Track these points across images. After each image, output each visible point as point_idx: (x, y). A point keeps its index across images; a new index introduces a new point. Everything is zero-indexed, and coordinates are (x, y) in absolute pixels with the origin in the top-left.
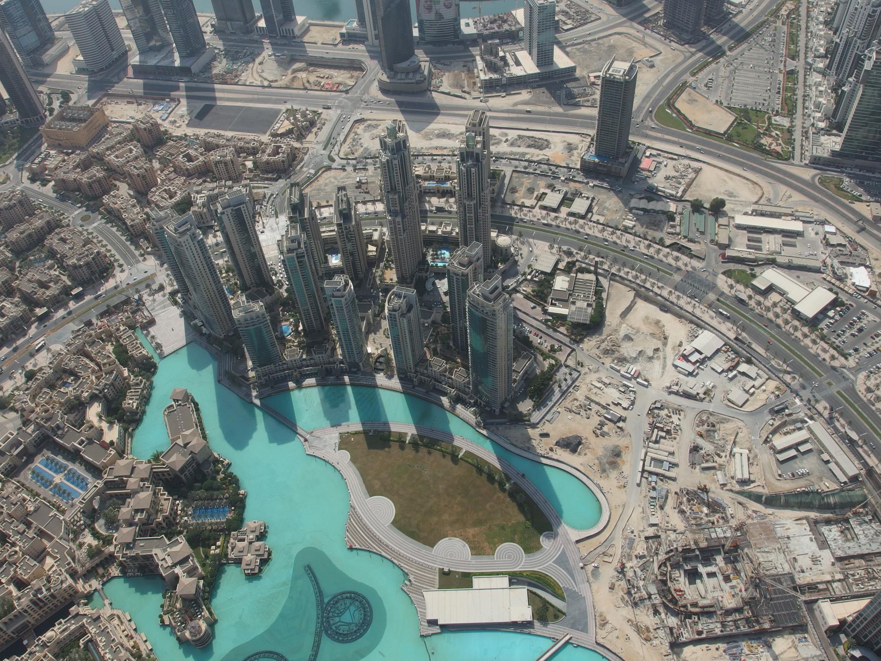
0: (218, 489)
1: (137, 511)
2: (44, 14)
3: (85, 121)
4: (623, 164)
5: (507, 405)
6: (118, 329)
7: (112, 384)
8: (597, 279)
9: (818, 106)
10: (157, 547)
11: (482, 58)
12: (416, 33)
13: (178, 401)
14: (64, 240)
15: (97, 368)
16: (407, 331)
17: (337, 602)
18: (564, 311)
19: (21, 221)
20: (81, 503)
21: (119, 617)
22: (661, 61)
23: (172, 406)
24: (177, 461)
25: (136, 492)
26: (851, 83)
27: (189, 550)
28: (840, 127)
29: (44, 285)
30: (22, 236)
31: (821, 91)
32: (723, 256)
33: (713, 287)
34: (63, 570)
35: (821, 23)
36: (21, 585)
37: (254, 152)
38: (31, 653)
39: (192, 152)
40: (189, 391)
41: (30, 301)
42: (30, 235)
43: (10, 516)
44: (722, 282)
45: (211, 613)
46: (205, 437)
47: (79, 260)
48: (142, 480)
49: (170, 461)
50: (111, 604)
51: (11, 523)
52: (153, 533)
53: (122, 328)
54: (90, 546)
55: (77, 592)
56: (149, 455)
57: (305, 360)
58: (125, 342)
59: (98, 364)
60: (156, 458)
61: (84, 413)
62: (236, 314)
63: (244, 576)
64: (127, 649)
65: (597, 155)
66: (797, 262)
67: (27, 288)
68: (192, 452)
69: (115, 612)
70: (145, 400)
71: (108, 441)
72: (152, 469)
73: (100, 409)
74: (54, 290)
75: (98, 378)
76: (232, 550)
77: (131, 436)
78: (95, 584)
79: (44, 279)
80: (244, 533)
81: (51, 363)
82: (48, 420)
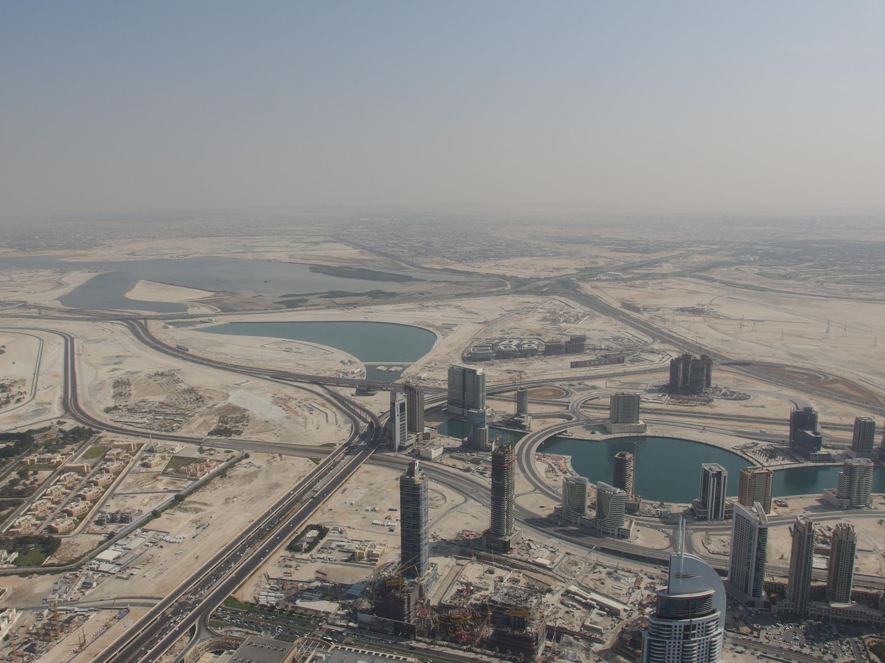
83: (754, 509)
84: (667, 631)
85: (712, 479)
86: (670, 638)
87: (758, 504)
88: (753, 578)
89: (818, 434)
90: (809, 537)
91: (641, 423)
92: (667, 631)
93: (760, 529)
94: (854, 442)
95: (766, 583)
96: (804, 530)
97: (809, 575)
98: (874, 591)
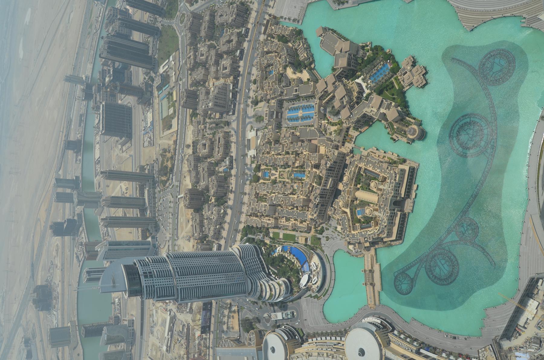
0: (375, 59)
1: (342, 99)
6: (272, 30)
7: (288, 54)
10: (364, 108)
14: (221, 16)
15: (276, 54)
17: (484, 64)
19: (201, 24)
20: (316, 116)
21: (373, 152)
23: (322, 40)
24: (343, 62)
25: (334, 91)
27: (380, 98)
29: (229, 41)
30: (206, 30)
34: (331, 149)
36: (317, 166)
38: (343, 191)
40: (324, 26)
41: (230, 53)
42: (209, 27)
43: (292, 143)
45: (414, 119)
46: (346, 40)
47: (232, 16)
48: (334, 84)
49: (339, 65)
50: (364, 149)
51: (294, 145)
52: (358, 103)
53: (273, 28)
54: (335, 131)
55: (344, 154)
56: (330, 71)
58: (279, 32)
59: (276, 52)
60: (334, 70)
61: (286, 77)
63: (421, 89)
64: (386, 162)
67: (224, 48)
68: (346, 52)
69: (369, 151)
70: (308, 48)
71: (307, 81)
72: (334, 75)
73: (292, 70)
74: (235, 39)
75: (280, 58)
76: (404, 81)
77: (314, 69)
78: (349, 146)
79: (228, 39)
80: (404, 69)
81: (257, 69)
82: (274, 93)
83: (99, 250)
84: (149, 288)
85: (92, 276)
86: (154, 286)
87: (96, 248)
88: (143, 246)
89: (65, 220)
90: (109, 219)
91: (69, 325)
92: (149, 288)
93: (110, 245)
94: (70, 202)
95: (142, 239)
96: (107, 222)
97: (135, 218)
98: (138, 186)
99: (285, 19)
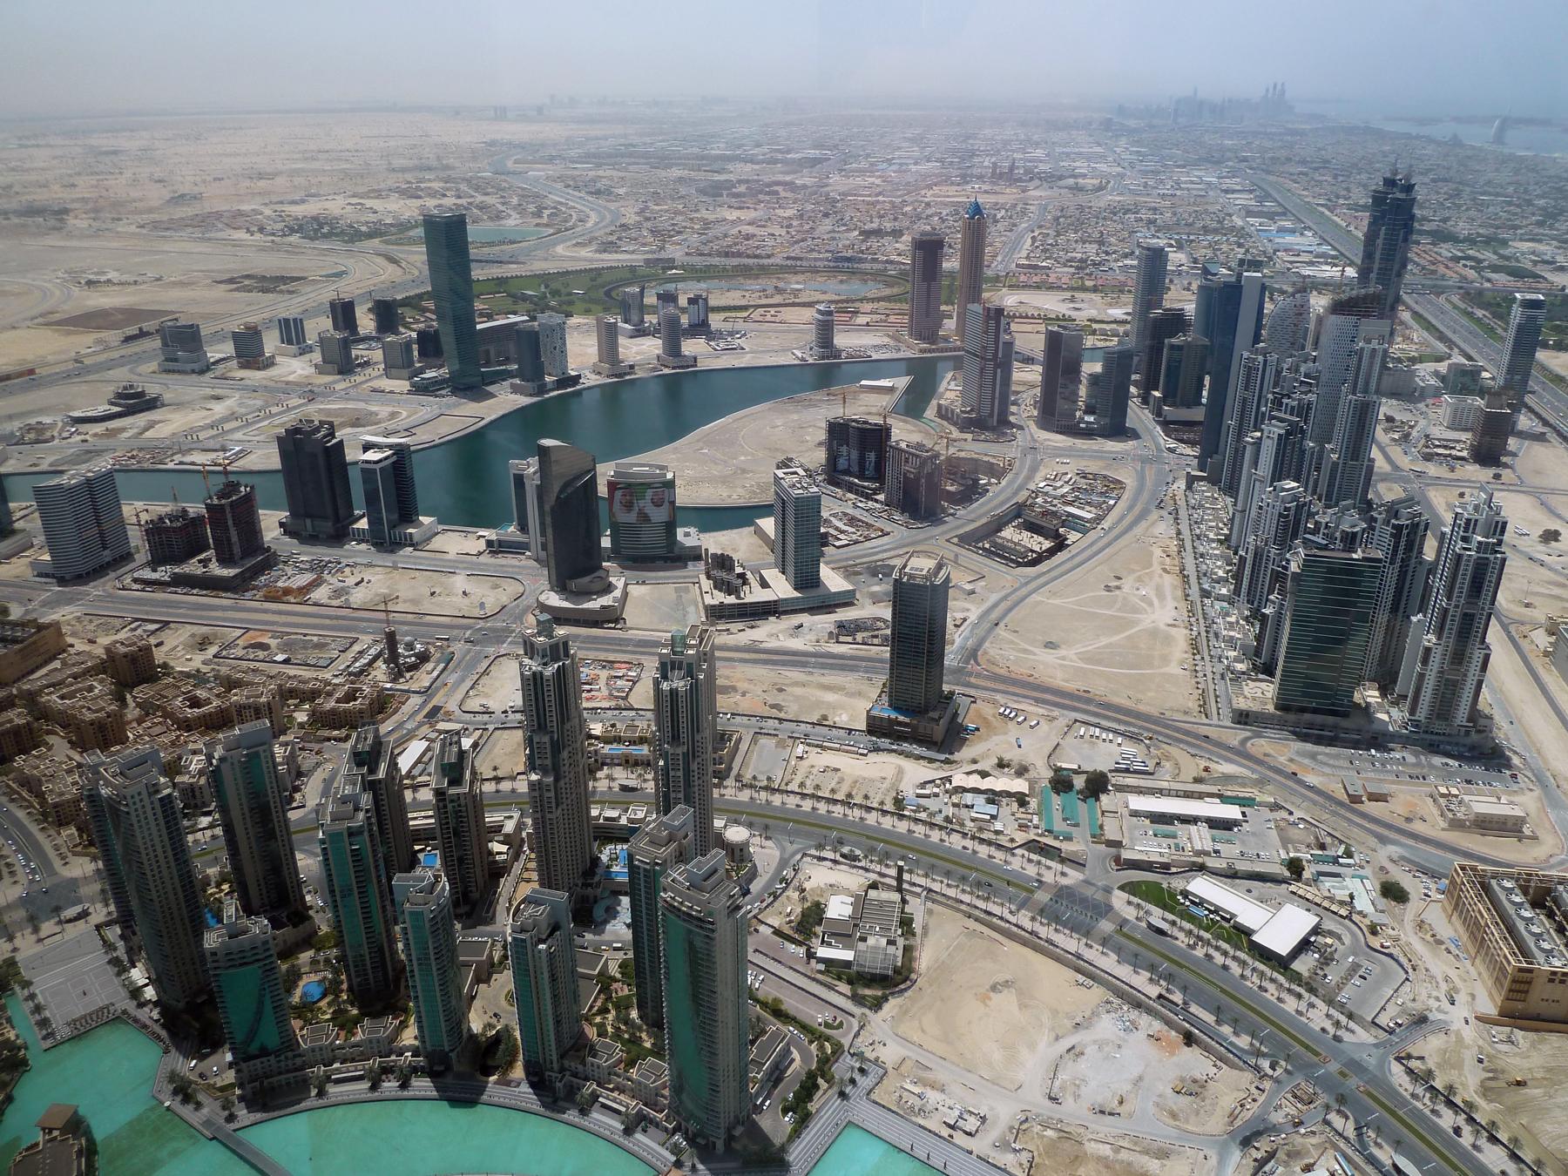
2: (5, 501)
3: (22, 642)
4: (937, 721)
5: (738, 1132)
8: (904, 901)
9: (1231, 642)
11: (709, 577)
12: (606, 542)
13: (51, 1130)
16: (546, 975)
18: (848, 955)
22: (982, 587)
23: (37, 1145)
26: (1274, 602)
28: (1269, 670)
31: (1230, 623)
32: (1117, 860)
33: (1106, 910)
35: (1213, 540)
37: (312, 695)
39: (201, 693)
40: (81, 1111)
44: (1119, 900)
57: (341, 1047)
62: (212, 940)
65: (894, 706)
66: (1242, 866)
99: (32, 997)
